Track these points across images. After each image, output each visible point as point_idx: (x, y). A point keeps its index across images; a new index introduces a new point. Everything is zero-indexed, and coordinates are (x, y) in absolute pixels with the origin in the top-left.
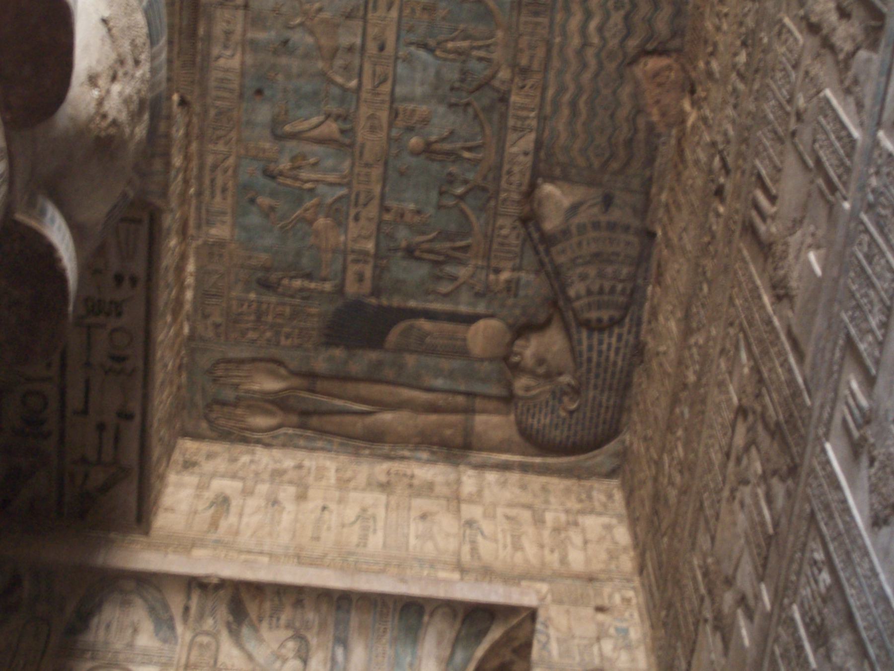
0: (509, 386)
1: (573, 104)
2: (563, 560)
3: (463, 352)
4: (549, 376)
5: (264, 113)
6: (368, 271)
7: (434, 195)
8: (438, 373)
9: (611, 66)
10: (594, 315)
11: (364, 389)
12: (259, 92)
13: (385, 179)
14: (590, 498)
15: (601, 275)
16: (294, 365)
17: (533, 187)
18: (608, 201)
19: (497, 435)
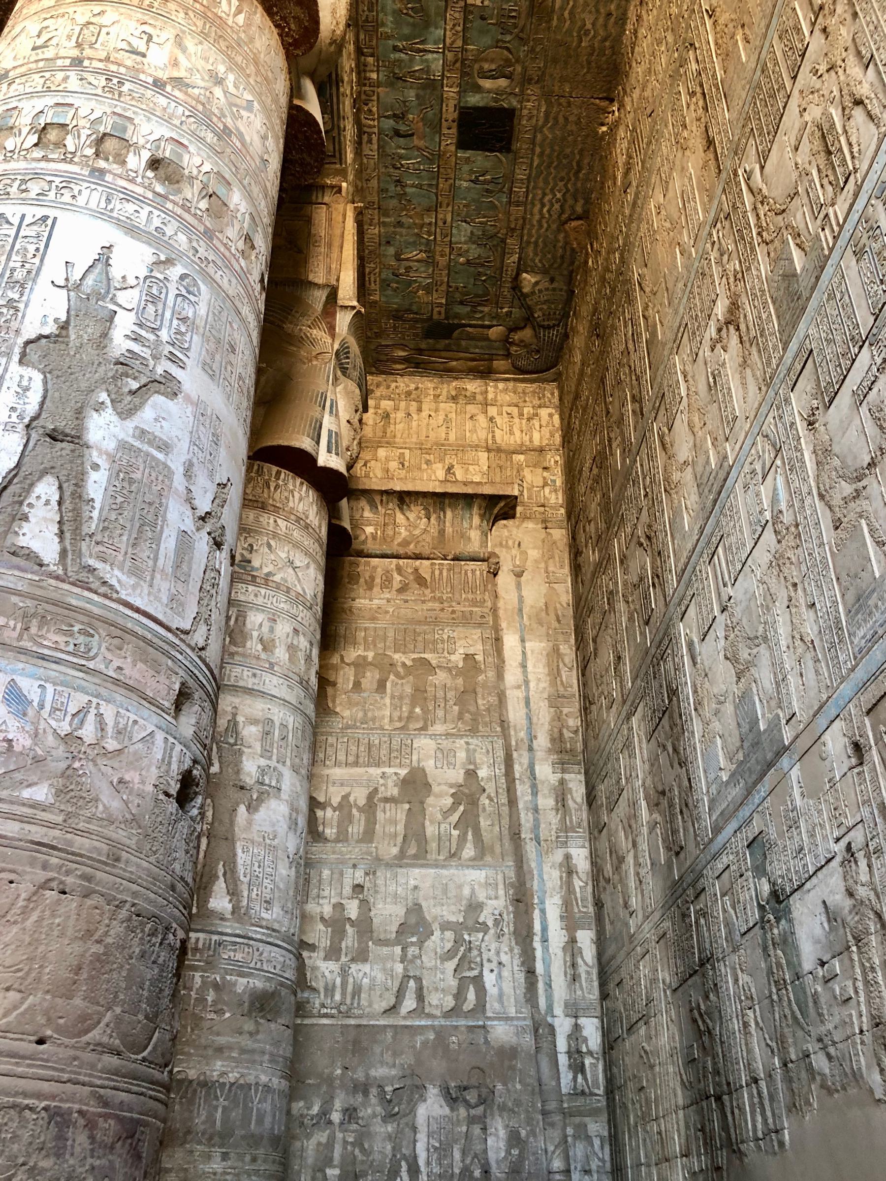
0: (508, 350)
1: (536, 243)
2: (531, 441)
3: (487, 339)
4: (525, 346)
5: (391, 250)
6: (443, 310)
7: (472, 280)
8: (476, 347)
9: (554, 226)
10: (546, 323)
11: (443, 354)
12: (388, 242)
13: (449, 275)
14: (544, 396)
15: (549, 308)
16: (412, 346)
17: (518, 274)
18: (552, 280)
19: (502, 369)
